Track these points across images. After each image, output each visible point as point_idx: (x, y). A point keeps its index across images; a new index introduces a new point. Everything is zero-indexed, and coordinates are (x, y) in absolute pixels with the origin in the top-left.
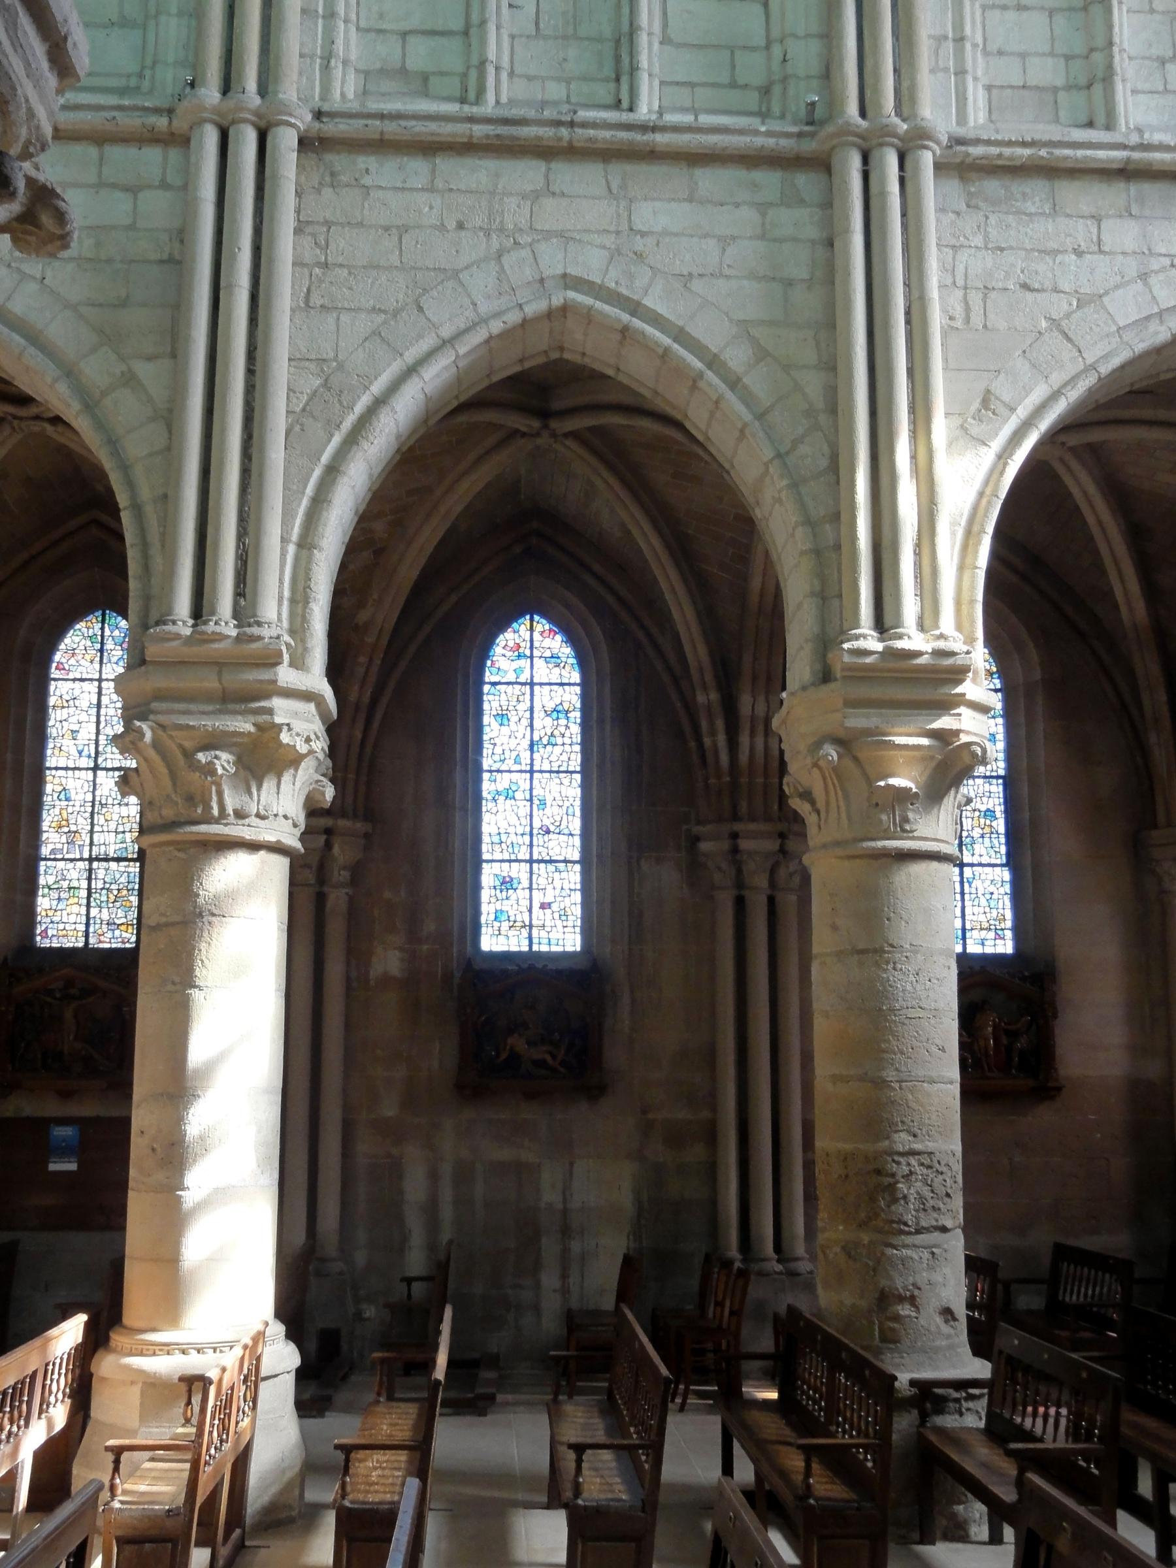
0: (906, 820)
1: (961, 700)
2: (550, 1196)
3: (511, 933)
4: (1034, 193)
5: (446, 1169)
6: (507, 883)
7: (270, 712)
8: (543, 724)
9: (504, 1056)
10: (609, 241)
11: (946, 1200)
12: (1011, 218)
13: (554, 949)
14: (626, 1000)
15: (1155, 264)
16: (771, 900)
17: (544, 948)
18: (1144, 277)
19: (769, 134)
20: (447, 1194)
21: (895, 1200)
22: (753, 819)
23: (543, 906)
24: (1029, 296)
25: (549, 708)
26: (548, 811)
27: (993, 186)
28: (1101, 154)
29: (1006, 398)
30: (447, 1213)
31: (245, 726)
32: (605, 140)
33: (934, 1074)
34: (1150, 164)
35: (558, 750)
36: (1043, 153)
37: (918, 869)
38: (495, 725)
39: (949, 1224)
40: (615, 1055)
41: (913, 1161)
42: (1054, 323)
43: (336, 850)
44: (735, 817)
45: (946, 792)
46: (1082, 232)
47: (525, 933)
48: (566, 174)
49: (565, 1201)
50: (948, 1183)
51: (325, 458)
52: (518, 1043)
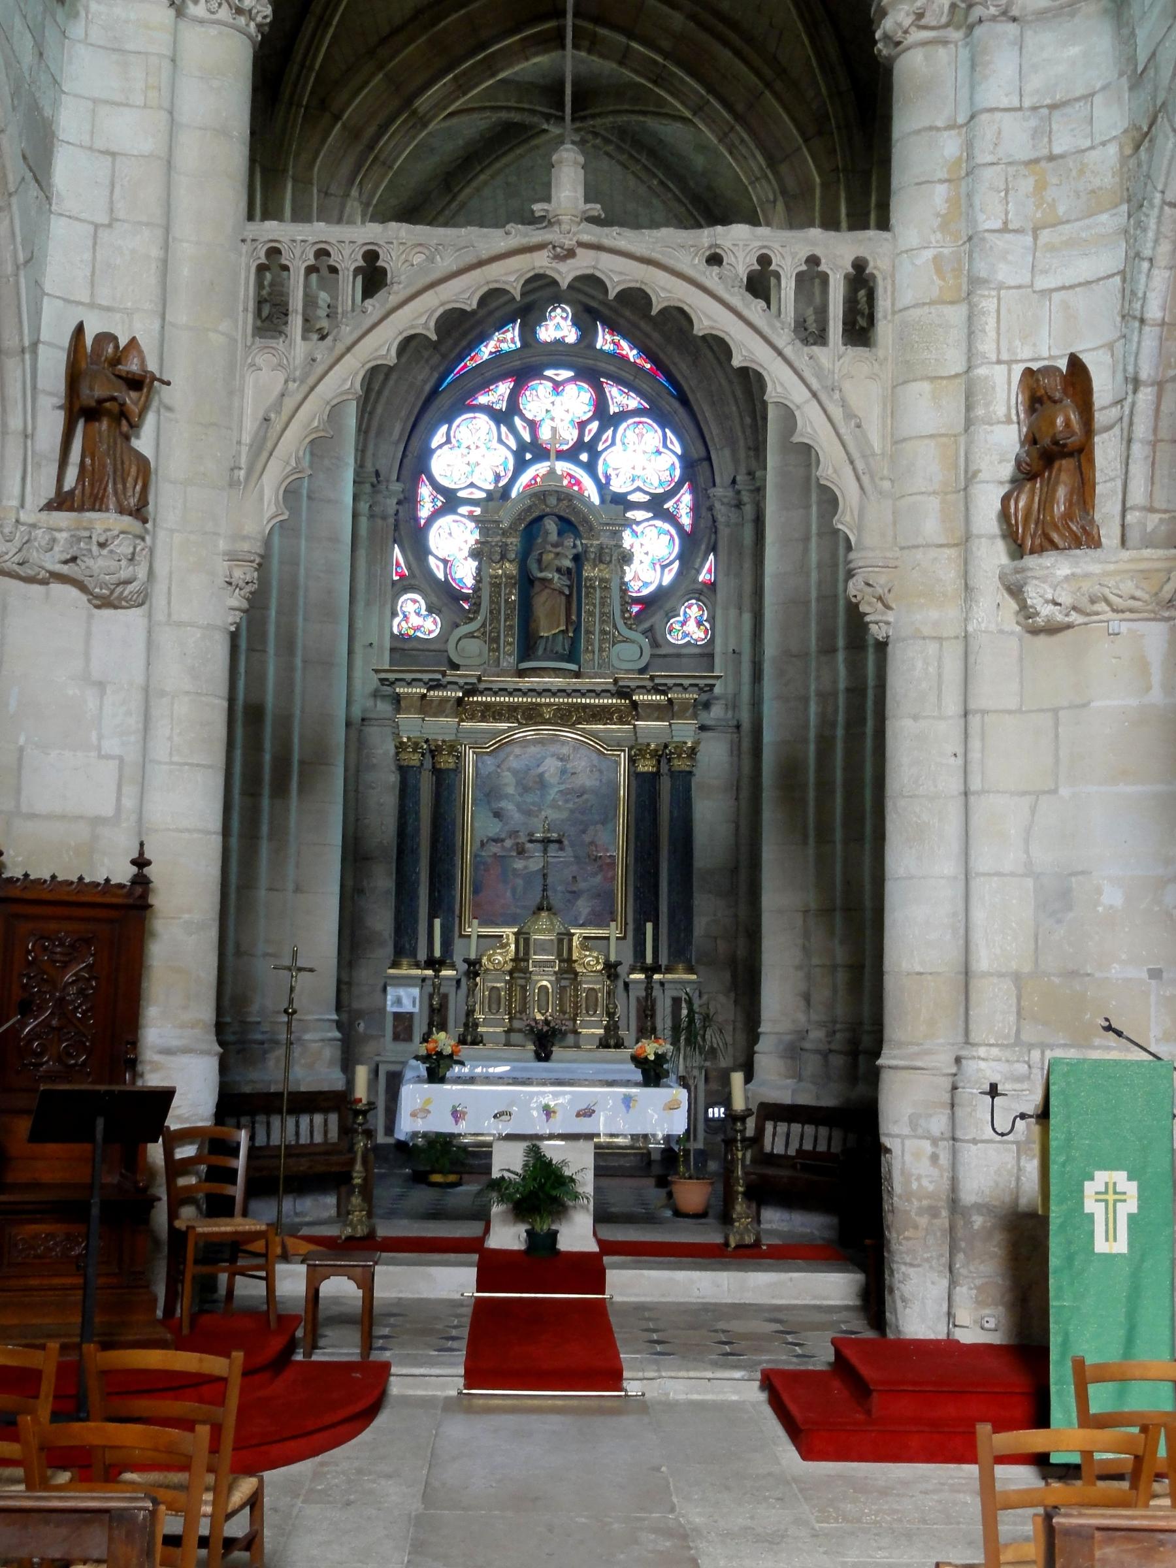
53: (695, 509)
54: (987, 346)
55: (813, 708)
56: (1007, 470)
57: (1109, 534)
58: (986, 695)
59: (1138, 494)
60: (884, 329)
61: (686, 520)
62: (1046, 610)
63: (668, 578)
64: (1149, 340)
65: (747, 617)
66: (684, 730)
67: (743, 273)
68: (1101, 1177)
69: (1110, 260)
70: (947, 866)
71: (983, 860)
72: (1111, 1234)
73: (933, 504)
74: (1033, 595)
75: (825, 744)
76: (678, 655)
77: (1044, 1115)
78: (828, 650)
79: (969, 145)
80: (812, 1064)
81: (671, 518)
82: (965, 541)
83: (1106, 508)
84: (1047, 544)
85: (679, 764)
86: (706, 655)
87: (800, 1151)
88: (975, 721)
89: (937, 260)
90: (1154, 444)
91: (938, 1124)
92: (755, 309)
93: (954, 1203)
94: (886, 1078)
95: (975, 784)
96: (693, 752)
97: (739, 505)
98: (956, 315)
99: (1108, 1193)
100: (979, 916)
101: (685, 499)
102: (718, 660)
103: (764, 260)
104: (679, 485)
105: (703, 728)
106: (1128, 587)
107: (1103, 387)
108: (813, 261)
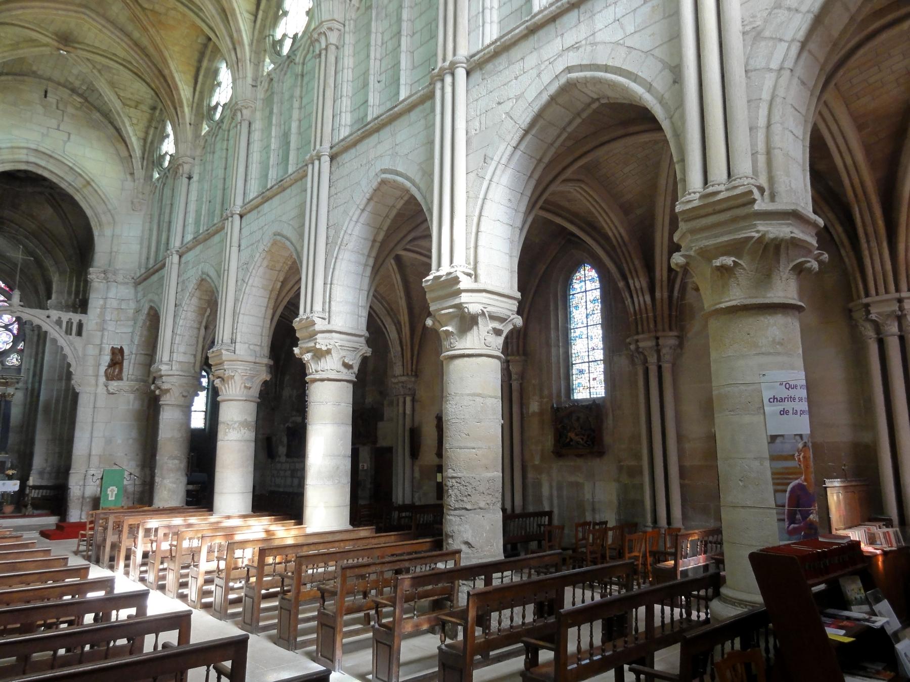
0: (451, 343)
1: (460, 292)
2: (588, 496)
3: (584, 391)
4: (503, 60)
5: (554, 484)
6: (581, 372)
7: (316, 339)
8: (590, 306)
9: (568, 440)
10: (390, 152)
11: (469, 497)
12: (495, 78)
13: (598, 396)
14: (611, 417)
15: (543, 67)
16: (660, 368)
17: (595, 396)
18: (539, 75)
19: (423, 89)
20: (555, 493)
21: (448, 497)
22: (643, 332)
23: (594, 379)
24: (500, 107)
25: (592, 299)
26: (594, 341)
27: (490, 66)
28: (517, 31)
29: (490, 156)
30: (555, 501)
31: (312, 344)
32: (386, 118)
33: (462, 445)
34: (535, 23)
35: (595, 316)
36: (498, 43)
37: (458, 362)
38: (574, 310)
39: (469, 507)
40: (608, 439)
41: (454, 481)
42: (507, 113)
43: (511, 367)
44: (637, 333)
45: (470, 328)
46: (517, 68)
47: (588, 390)
48: (382, 133)
49: (593, 498)
50: (469, 490)
51: (335, 256)
52: (572, 435)
53: (19, 329)
54: (105, 341)
55: (55, 393)
56: (107, 364)
57: (125, 378)
58: (99, 404)
59: (131, 372)
60: (84, 333)
61: (15, 332)
62: (112, 391)
63: (8, 347)
64: (135, 348)
65: (33, 360)
66: (11, 390)
67: (55, 320)
68: (111, 488)
69: (130, 330)
70: (87, 435)
71: (95, 434)
72: (112, 497)
73: (91, 368)
74: (109, 388)
75: (57, 401)
76: (10, 368)
77: (102, 478)
78: (60, 379)
79: (105, 303)
80: (46, 476)
81: (10, 331)
82: (97, 376)
83: (125, 374)
84: (112, 379)
85: (8, 399)
86: (18, 369)
87: (42, 496)
88: (96, 409)
89: (97, 323)
90: (134, 364)
91: (81, 483)
92: (57, 328)
93: (83, 497)
94: (71, 475)
95: (95, 420)
96: (13, 395)
97: (33, 330)
98: (99, 333)
99: (112, 491)
100: (93, 444)
101: (16, 326)
102: (23, 371)
103: (60, 318)
104: (14, 322)
105: (16, 389)
106: (127, 388)
107: (126, 352)
108: (70, 319)
